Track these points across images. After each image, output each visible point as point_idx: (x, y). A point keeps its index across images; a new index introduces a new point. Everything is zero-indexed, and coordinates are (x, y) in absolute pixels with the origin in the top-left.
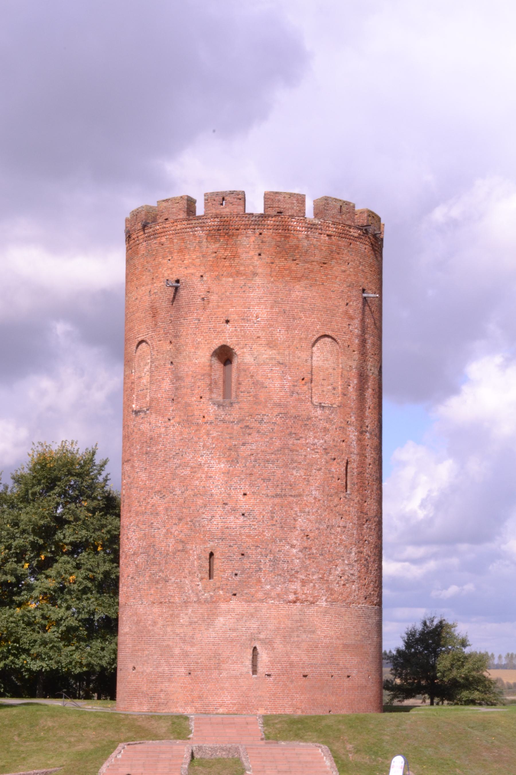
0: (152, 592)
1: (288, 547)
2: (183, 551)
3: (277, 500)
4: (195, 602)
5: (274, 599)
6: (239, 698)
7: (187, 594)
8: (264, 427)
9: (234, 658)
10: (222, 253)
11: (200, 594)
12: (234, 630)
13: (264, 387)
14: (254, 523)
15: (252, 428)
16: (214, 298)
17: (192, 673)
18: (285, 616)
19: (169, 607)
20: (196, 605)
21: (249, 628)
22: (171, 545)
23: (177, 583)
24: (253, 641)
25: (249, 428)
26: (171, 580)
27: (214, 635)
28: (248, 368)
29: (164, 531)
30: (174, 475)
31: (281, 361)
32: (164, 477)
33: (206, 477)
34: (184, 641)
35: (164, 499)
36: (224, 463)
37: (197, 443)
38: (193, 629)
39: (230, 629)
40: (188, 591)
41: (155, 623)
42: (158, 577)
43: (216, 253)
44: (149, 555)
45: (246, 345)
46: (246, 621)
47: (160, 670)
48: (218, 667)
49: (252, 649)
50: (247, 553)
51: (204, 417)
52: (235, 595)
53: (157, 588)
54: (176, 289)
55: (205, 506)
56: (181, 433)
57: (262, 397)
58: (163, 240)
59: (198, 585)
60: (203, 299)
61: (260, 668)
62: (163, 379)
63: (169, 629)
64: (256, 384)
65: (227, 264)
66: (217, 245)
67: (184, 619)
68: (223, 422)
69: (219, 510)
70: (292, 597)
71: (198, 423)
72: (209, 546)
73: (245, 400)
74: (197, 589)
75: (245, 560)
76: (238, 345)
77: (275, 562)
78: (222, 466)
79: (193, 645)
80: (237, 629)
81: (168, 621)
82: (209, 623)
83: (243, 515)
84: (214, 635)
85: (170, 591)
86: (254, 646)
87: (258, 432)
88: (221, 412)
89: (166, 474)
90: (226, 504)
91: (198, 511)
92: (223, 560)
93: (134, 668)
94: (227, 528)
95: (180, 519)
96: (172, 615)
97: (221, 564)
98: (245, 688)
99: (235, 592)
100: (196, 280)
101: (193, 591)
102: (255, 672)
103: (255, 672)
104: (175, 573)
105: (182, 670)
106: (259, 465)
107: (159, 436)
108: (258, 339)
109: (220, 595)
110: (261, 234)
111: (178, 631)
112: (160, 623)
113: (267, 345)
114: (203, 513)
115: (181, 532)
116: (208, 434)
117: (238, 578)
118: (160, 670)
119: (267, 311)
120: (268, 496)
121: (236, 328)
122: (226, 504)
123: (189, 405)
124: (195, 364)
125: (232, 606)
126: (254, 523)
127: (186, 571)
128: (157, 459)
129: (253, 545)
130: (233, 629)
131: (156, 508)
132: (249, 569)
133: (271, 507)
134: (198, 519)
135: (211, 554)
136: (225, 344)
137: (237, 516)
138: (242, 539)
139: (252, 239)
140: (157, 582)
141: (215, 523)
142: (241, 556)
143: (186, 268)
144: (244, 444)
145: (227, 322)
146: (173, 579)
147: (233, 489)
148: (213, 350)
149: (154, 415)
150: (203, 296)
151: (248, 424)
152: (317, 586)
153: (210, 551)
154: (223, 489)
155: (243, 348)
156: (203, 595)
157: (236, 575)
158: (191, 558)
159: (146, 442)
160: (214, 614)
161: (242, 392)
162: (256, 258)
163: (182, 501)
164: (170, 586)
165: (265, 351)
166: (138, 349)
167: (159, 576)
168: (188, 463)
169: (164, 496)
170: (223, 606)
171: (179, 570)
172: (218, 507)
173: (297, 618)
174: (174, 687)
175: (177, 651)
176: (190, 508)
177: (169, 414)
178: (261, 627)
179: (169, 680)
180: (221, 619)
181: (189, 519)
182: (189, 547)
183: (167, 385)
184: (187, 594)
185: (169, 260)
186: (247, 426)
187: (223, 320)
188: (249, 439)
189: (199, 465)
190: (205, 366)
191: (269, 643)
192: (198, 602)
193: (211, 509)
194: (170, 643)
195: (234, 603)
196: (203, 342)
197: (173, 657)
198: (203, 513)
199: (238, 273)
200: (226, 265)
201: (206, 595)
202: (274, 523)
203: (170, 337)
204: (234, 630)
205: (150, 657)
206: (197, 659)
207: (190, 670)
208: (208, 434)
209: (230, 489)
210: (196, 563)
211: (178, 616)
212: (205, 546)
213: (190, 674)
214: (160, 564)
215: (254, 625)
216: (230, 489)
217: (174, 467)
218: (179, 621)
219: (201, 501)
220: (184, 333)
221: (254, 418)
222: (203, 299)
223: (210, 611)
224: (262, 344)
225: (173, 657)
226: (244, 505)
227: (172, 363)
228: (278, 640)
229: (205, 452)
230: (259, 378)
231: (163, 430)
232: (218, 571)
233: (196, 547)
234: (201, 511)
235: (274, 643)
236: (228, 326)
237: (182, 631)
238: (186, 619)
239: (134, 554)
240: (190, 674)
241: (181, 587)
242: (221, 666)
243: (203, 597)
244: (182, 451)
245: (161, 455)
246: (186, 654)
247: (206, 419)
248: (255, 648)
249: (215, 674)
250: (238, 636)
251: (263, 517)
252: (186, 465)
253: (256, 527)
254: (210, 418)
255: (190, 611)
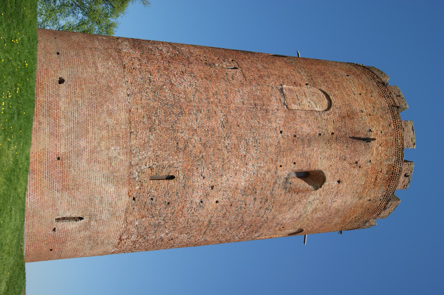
0: (140, 111)
1: (167, 232)
2: (178, 148)
3: (206, 223)
4: (131, 162)
5: (125, 227)
6: (32, 209)
7: (138, 154)
8: (263, 211)
9: (74, 203)
10: (380, 176)
11: (137, 167)
12: (101, 202)
13: (290, 209)
14: (193, 210)
15: (264, 204)
16: (356, 171)
17: (60, 161)
18: (109, 236)
19: (126, 133)
20: (127, 164)
21: (101, 212)
22: (183, 135)
23: (148, 142)
24: (88, 217)
25: (265, 202)
26: (152, 134)
27: (98, 183)
28: (306, 198)
29: (195, 127)
30: (240, 138)
31: (301, 217)
32: (238, 126)
33: (237, 170)
34: (92, 152)
35: (221, 127)
36: (244, 185)
37: (263, 161)
38: (105, 162)
39: (102, 197)
40: (141, 156)
41: (110, 114)
42: (154, 118)
43: (381, 172)
44: (172, 106)
45: (321, 195)
46: (108, 210)
47: (63, 122)
48: (65, 188)
49: (82, 217)
50: (169, 207)
51: (281, 166)
52: (134, 199)
53: (144, 117)
54: (364, 139)
55: (214, 170)
56: (271, 145)
57: (285, 208)
58: (393, 127)
59: (146, 165)
60: (357, 163)
61: (62, 223)
62: (309, 126)
63: (104, 133)
64: (294, 204)
65: (373, 180)
66: (385, 172)
67: (114, 151)
68: (274, 183)
69: (208, 183)
70: (124, 237)
71: (277, 161)
72: (180, 174)
73: (286, 198)
74: (142, 164)
75: (163, 206)
76: (323, 190)
77: (159, 225)
78: (243, 184)
79: (89, 161)
80: (101, 204)
81: (112, 132)
82: (110, 178)
83: (202, 202)
84: (98, 183)
85: (141, 133)
86: (84, 218)
87: (261, 208)
88: (282, 180)
89: (241, 128)
90: (212, 188)
91: (210, 163)
92: (166, 189)
93: (61, 81)
94: (193, 190)
95: (204, 145)
96: (118, 136)
97: (163, 186)
98: (43, 214)
99: (137, 199)
100: (368, 157)
101: (140, 160)
102: (58, 220)
103: (58, 220)
104: (157, 140)
105: (62, 150)
106: (236, 210)
107: (270, 121)
108: (321, 203)
109: (135, 186)
110: (381, 200)
111: (103, 144)
112: (111, 122)
113: (316, 209)
114: (208, 169)
115: (194, 147)
116: (269, 170)
117: (149, 201)
118: (63, 122)
119: (335, 207)
120: (212, 217)
121: (334, 188)
122: (212, 188)
123: (291, 152)
124: (317, 157)
125: (123, 198)
126: (193, 210)
127: (159, 153)
128: (252, 119)
129: (175, 211)
130: (102, 200)
131: (213, 117)
132: (155, 210)
133: (202, 220)
134: (204, 163)
135: (172, 178)
136: (326, 181)
137: (201, 198)
138: (182, 203)
139: (380, 195)
140: (149, 118)
141: (199, 179)
142: (167, 202)
143: (377, 148)
144: (255, 199)
145: (339, 182)
146: (151, 137)
147: (223, 193)
148: (324, 172)
149: (284, 115)
150: (358, 163)
151: (268, 201)
152: (129, 247)
153: (176, 176)
154: (225, 185)
155: (320, 194)
156: (137, 171)
157: (152, 199)
158: (171, 157)
159: (264, 105)
160: (118, 182)
161: (292, 195)
162: (369, 198)
163: (220, 147)
164: (146, 134)
165: (312, 208)
166: (320, 92)
167: (155, 120)
168: (249, 153)
169: (224, 127)
170: (125, 190)
171: (160, 145)
172: (212, 181)
173: (106, 242)
174: (44, 139)
175: (83, 143)
176: (214, 156)
177: (285, 132)
178: (102, 222)
179: (51, 134)
180: (112, 189)
181: (204, 154)
182: (181, 155)
183: (306, 129)
184: (138, 154)
185: (381, 132)
186: (267, 200)
187: (341, 179)
188: (258, 202)
189: (246, 163)
190: (315, 166)
191: (86, 227)
192: (131, 165)
193: (210, 176)
194: (90, 135)
195: (126, 199)
196: (331, 164)
197: (76, 139)
198: (208, 169)
199: (365, 188)
200: (372, 179)
201: (137, 173)
202: (189, 223)
203: (336, 133)
204: (101, 202)
205: (75, 108)
206: (73, 167)
207: (62, 159)
208: (269, 170)
209: (224, 191)
210: (166, 162)
211: (117, 143)
212: (180, 172)
213: (59, 159)
214: (165, 121)
215: (105, 216)
216: (224, 191)
217: (246, 138)
218: (112, 145)
219: (218, 166)
220: (338, 147)
221: (271, 204)
222: (357, 163)
223: (121, 179)
224: (317, 205)
225: (76, 139)
226: (210, 203)
227: (320, 134)
228: (88, 233)
229: (256, 168)
230: (297, 205)
231: (274, 125)
232: (157, 184)
233: (180, 162)
234: (210, 166)
235: (85, 231)
236: (336, 183)
237: (103, 148)
238: (115, 154)
239: (172, 84)
240: (59, 159)
241: (144, 146)
242: (66, 191)
243: (135, 171)
244: (258, 146)
245: (254, 122)
246: (79, 154)
247: (279, 168)
248: (81, 219)
249: (58, 186)
250: (95, 204)
251: (196, 216)
252: (247, 151)
253: (189, 212)
254: (280, 173)
255: (122, 158)
